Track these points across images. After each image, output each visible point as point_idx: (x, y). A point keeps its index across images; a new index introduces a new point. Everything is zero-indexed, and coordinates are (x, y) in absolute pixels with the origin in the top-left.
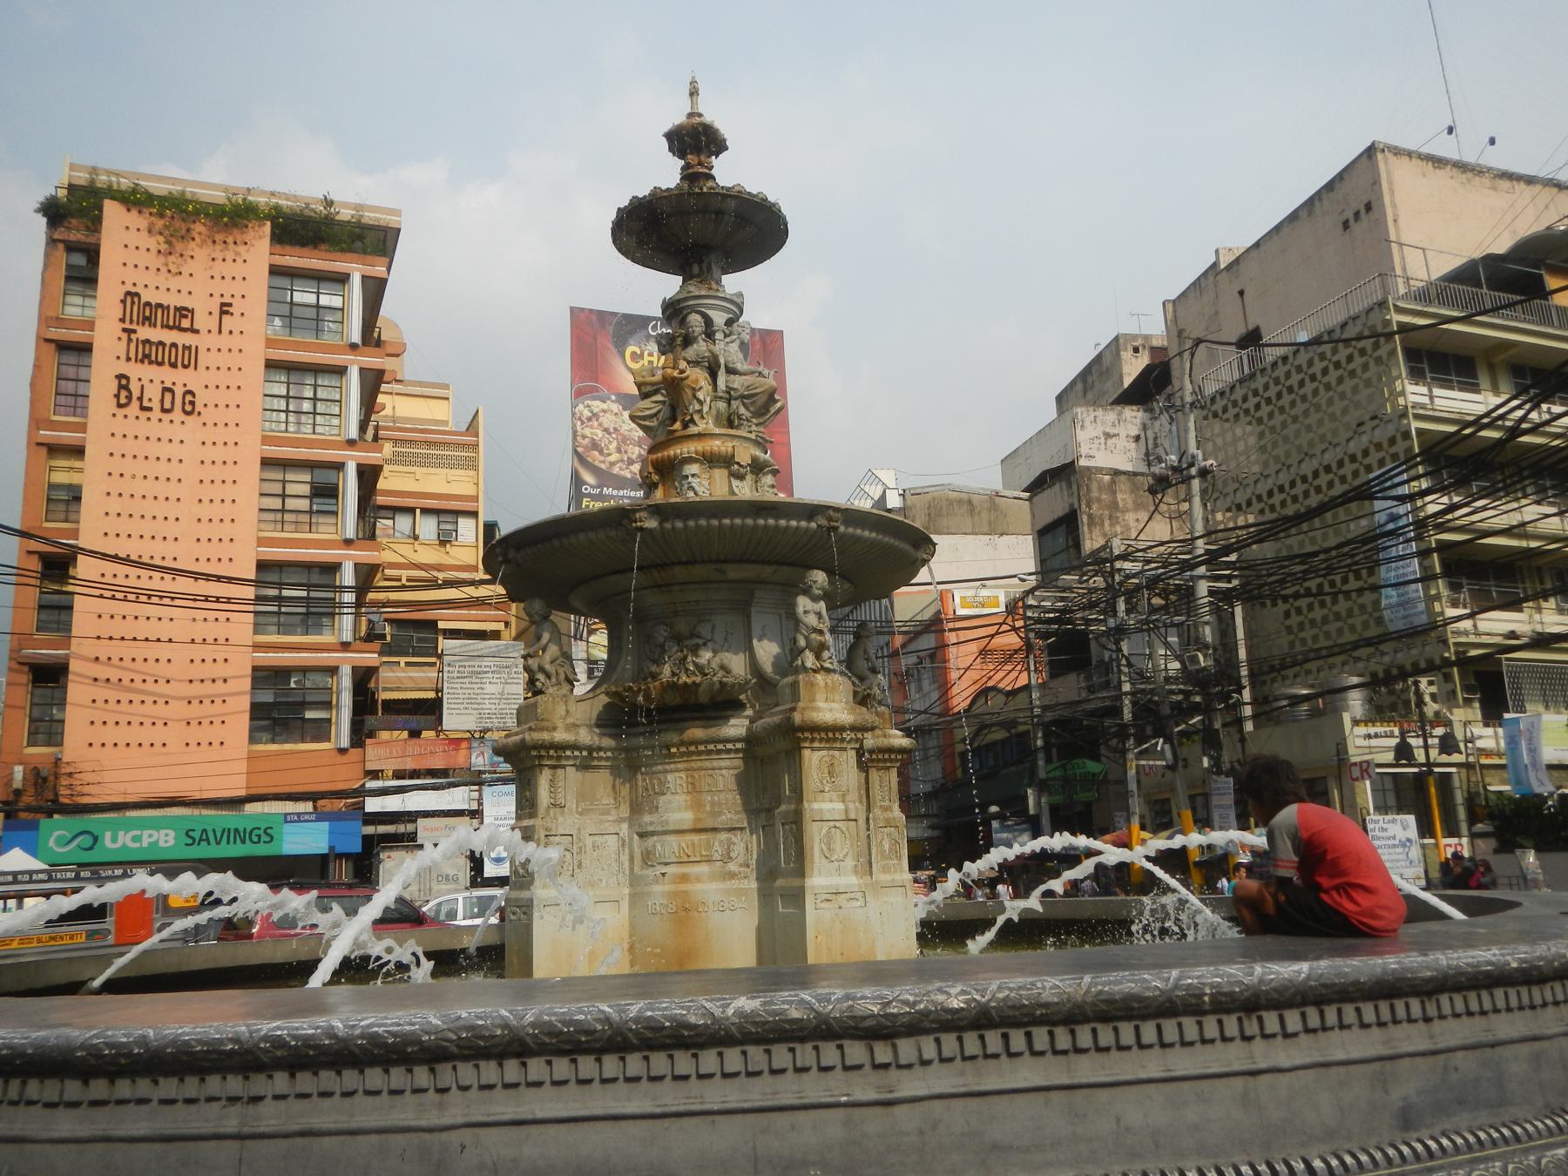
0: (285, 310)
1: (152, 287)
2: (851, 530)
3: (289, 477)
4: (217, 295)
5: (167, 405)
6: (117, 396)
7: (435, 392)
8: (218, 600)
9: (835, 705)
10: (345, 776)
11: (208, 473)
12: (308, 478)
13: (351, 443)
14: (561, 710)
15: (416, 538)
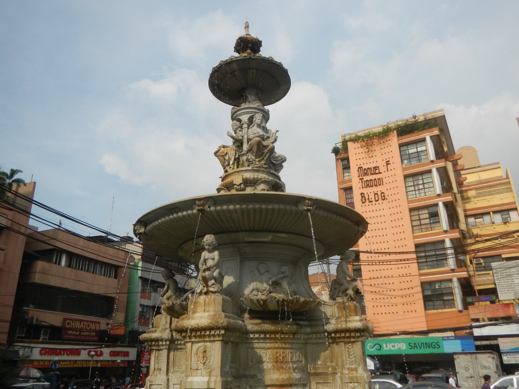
0: (407, 157)
1: (365, 163)
2: (218, 208)
3: (421, 212)
5: (377, 199)
6: (362, 200)
7: (496, 166)
8: (404, 260)
9: (206, 314)
10: (464, 322)
11: (393, 217)
12: (426, 211)
13: (439, 195)
14: (163, 321)
15: (493, 223)
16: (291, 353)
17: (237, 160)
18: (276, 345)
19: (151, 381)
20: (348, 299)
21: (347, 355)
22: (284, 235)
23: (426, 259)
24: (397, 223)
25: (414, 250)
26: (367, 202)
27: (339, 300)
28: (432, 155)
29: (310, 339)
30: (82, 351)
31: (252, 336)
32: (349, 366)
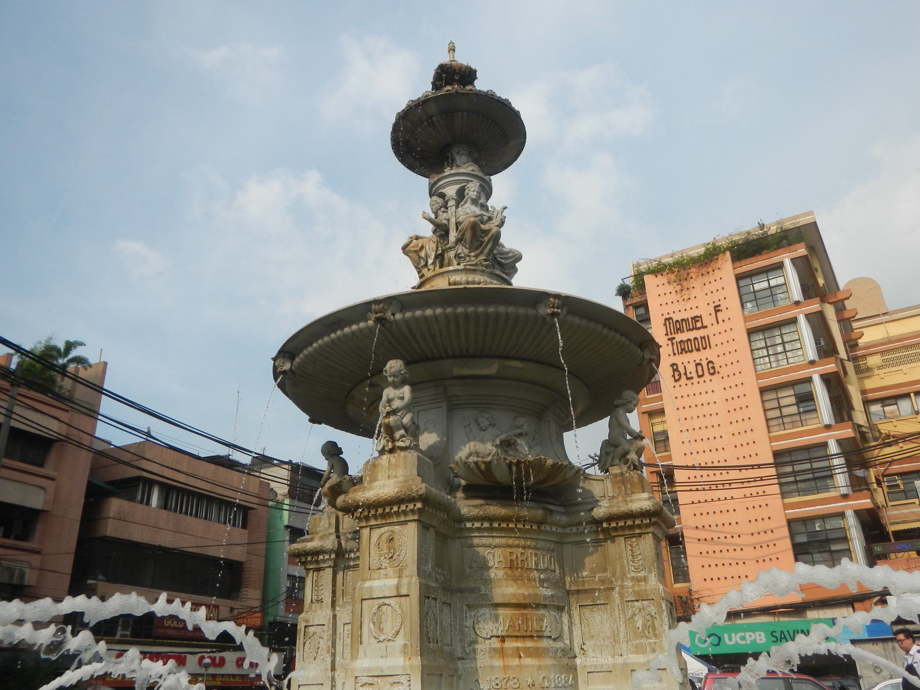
0: (752, 296)
1: (677, 311)
2: (408, 315)
3: (780, 395)
4: (711, 303)
5: (700, 373)
6: (674, 376)
9: (392, 481)
11: (732, 405)
12: (792, 392)
13: (812, 363)
16: (536, 555)
17: (440, 258)
18: (510, 541)
19: (306, 621)
20: (629, 468)
21: (630, 558)
22: (517, 364)
23: (795, 476)
24: (739, 415)
25: (772, 461)
26: (684, 380)
27: (615, 470)
28: (796, 292)
29: (567, 534)
30: (189, 656)
31: (469, 525)
32: (633, 574)
